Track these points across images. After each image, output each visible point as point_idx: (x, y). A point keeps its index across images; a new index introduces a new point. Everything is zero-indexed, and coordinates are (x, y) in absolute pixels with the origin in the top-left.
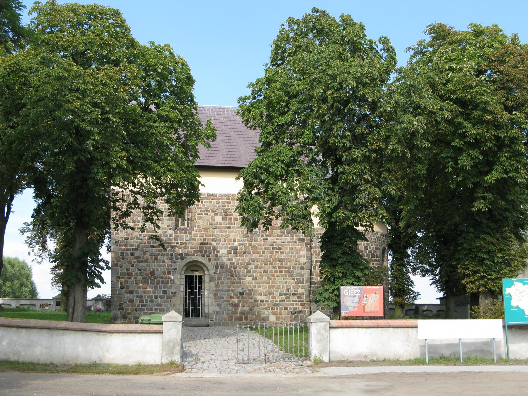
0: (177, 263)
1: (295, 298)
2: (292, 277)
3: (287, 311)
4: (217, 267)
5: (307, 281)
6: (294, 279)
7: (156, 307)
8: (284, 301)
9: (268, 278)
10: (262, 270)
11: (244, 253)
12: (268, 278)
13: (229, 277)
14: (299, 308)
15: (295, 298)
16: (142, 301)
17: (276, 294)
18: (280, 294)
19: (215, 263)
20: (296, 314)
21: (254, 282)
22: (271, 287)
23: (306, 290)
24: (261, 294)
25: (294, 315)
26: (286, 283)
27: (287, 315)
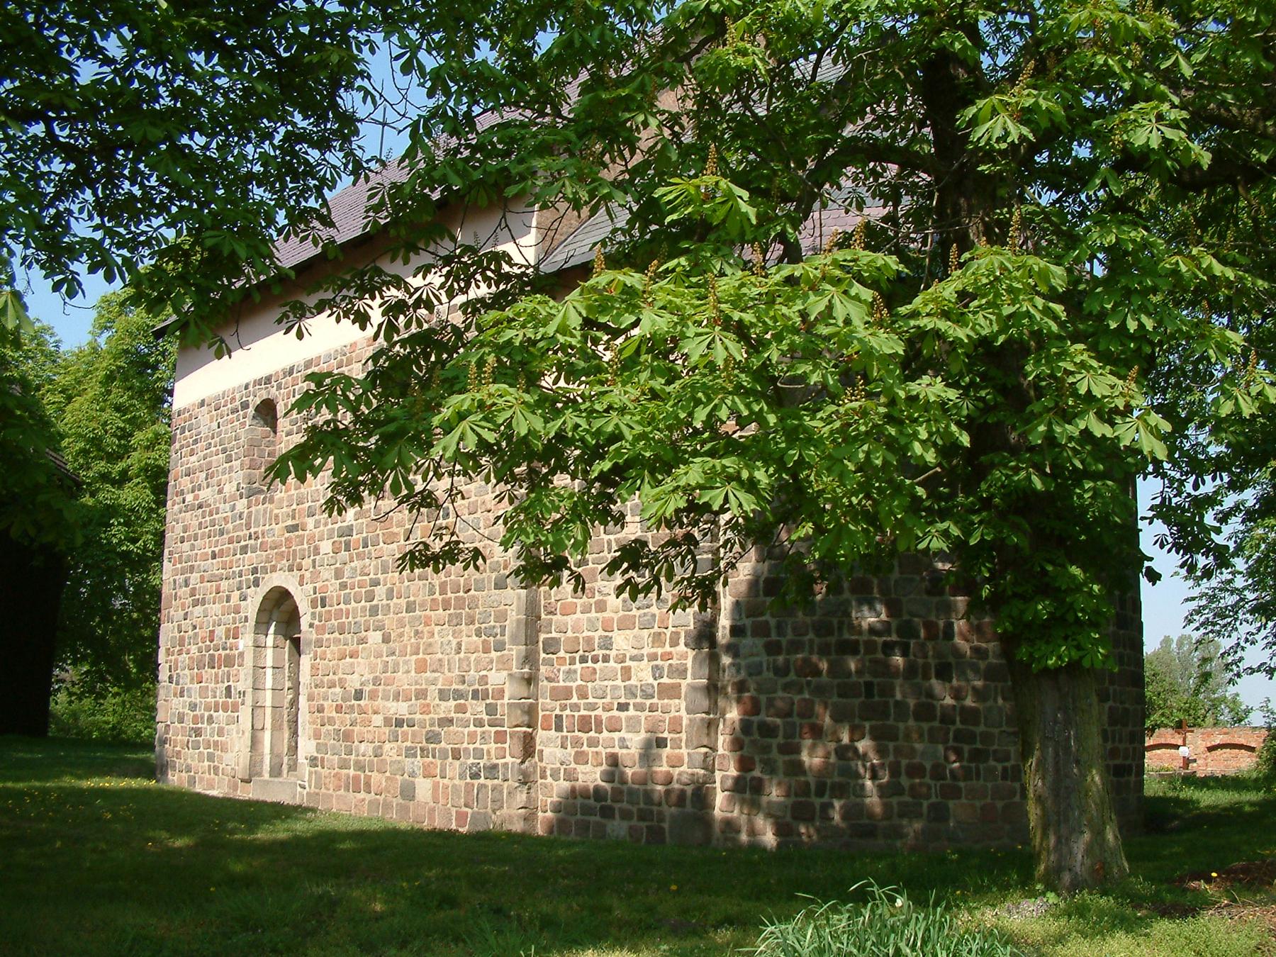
0: (249, 599)
1: (480, 707)
2: (472, 623)
3: (457, 763)
4: (314, 604)
5: (514, 640)
6: (478, 635)
7: (216, 738)
8: (451, 721)
9: (417, 632)
10: (403, 602)
11: (366, 546)
12: (417, 632)
13: (336, 635)
14: (489, 752)
15: (480, 707)
16: (196, 720)
17: (433, 691)
18: (443, 695)
19: (310, 587)
20: (482, 780)
21: (384, 647)
22: (421, 667)
23: (510, 675)
24: (397, 698)
25: (476, 782)
26: (459, 644)
27: (457, 782)
